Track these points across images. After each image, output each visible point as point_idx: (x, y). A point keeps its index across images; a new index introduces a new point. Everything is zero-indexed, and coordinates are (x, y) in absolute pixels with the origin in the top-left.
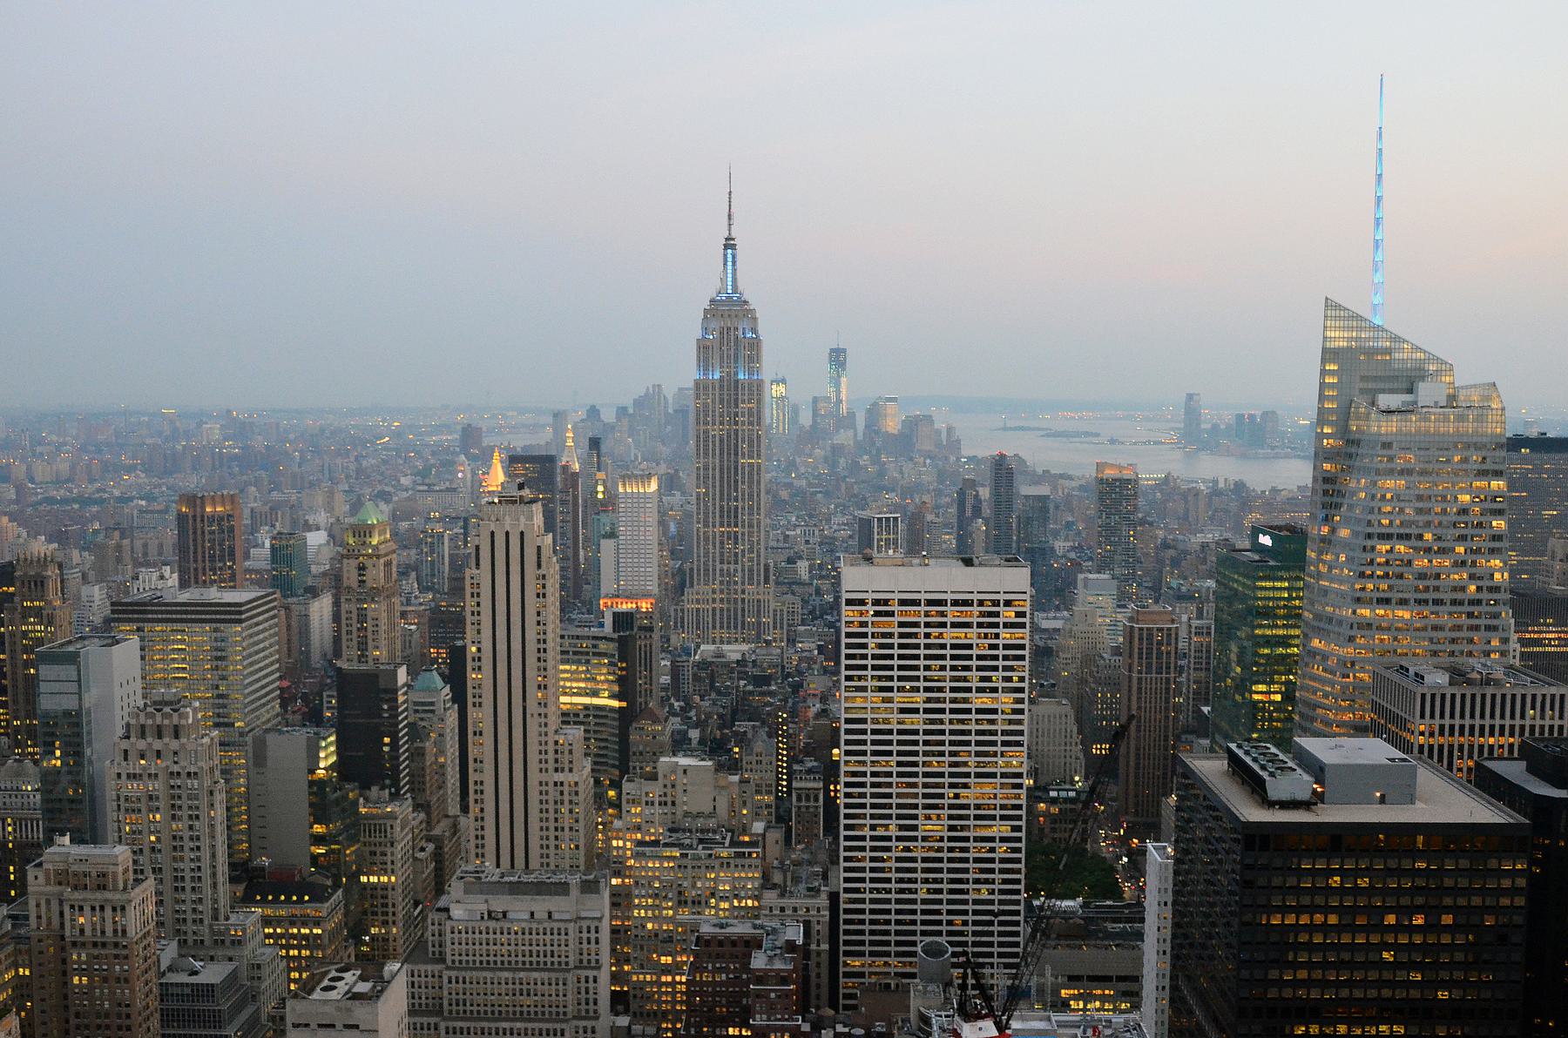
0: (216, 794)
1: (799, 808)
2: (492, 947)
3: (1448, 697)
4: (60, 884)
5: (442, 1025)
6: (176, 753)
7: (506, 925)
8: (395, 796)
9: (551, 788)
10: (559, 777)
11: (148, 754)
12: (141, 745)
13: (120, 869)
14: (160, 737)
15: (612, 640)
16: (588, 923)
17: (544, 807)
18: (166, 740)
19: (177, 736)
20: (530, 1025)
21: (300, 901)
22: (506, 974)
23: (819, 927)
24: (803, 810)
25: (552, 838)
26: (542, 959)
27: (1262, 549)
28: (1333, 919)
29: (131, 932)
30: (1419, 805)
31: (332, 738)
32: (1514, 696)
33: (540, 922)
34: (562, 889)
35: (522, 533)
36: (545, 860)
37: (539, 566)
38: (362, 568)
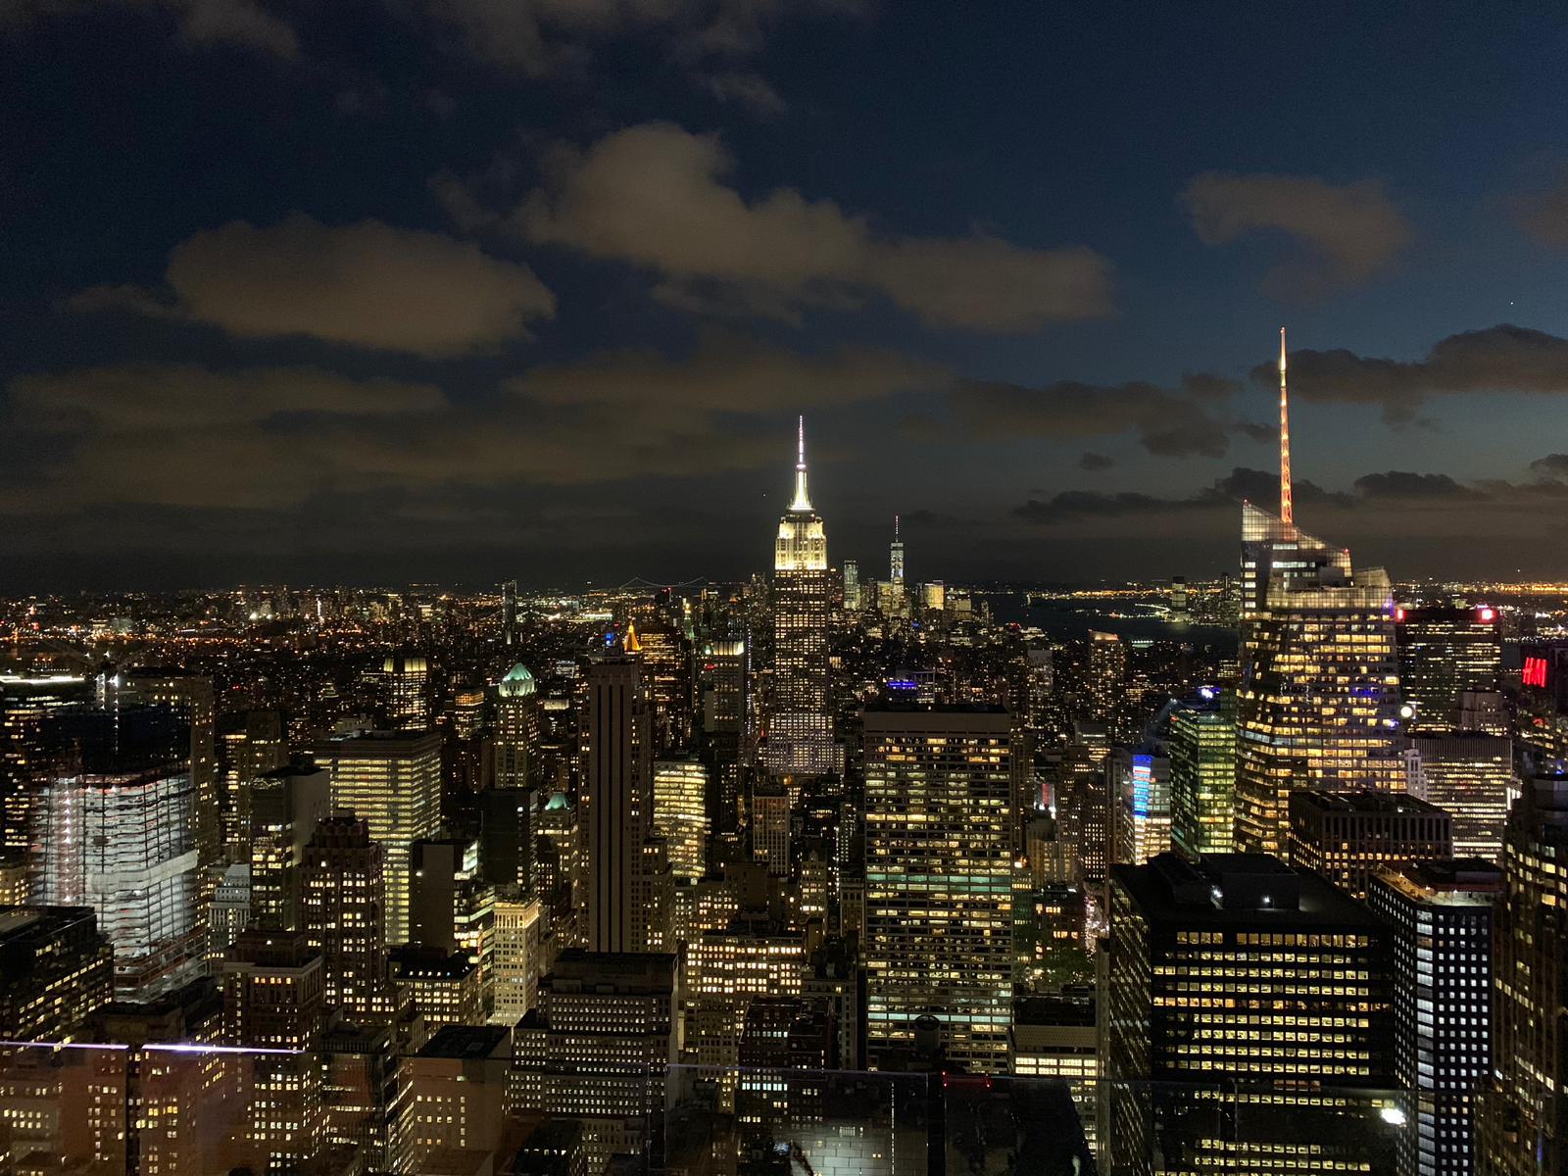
1: (845, 905)
3: (1349, 820)
9: (641, 887)
19: (350, 846)
21: (443, 978)
23: (846, 1003)
24: (849, 906)
25: (641, 927)
27: (1203, 700)
28: (1230, 1003)
30: (1301, 908)
31: (474, 847)
32: (1405, 820)
35: (622, 687)
36: (635, 945)
37: (634, 713)
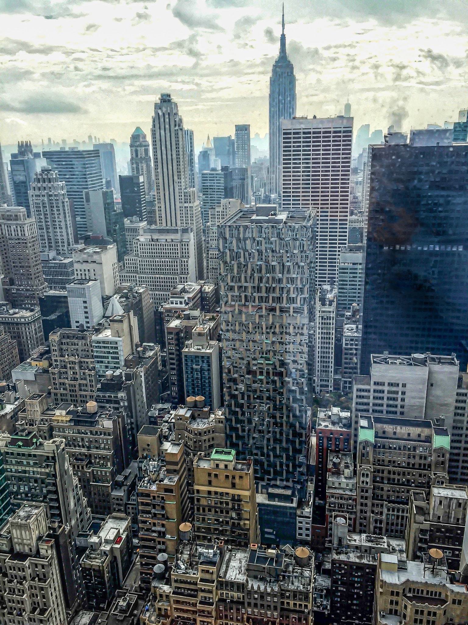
0: (66, 204)
2: (153, 251)
4: (4, 219)
5: (137, 276)
6: (50, 188)
7: (157, 243)
8: (141, 221)
9: (184, 209)
10: (186, 205)
11: (42, 188)
12: (39, 185)
13: (21, 214)
14: (45, 182)
15: (222, 175)
16: (184, 243)
17: (182, 215)
18: (47, 183)
20: (165, 276)
22: (157, 260)
26: (170, 255)
29: (27, 234)
33: (168, 242)
34: (176, 231)
38: (136, 151)
